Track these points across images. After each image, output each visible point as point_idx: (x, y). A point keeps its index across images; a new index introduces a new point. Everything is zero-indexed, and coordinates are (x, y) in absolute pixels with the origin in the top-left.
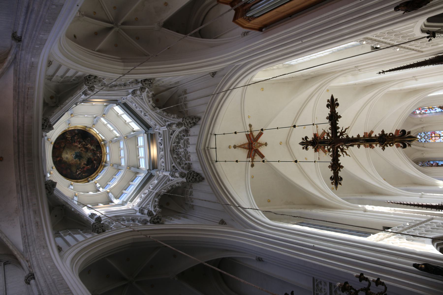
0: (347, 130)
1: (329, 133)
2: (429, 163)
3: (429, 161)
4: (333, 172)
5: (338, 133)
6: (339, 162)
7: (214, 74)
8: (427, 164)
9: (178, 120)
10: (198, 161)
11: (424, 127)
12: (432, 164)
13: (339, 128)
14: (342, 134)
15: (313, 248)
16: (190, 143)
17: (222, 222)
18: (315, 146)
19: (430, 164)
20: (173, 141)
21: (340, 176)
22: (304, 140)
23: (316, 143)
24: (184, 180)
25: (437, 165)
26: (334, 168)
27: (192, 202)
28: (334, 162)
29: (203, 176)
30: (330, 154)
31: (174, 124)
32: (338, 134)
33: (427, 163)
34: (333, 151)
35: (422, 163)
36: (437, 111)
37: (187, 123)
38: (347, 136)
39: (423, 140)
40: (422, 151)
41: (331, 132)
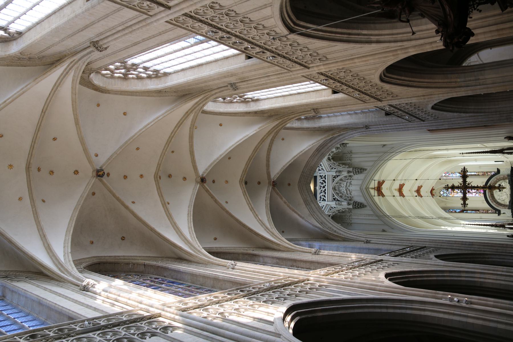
3: (449, 210)
7: (384, 145)
9: (347, 169)
10: (361, 194)
13: (467, 182)
14: (469, 184)
15: (454, 236)
16: (352, 184)
17: (384, 231)
20: (337, 182)
24: (351, 207)
25: (456, 212)
27: (351, 221)
29: (366, 204)
31: (342, 171)
32: (467, 184)
34: (463, 192)
36: (457, 175)
37: (356, 171)
38: (472, 185)
39: (445, 195)
40: (445, 202)
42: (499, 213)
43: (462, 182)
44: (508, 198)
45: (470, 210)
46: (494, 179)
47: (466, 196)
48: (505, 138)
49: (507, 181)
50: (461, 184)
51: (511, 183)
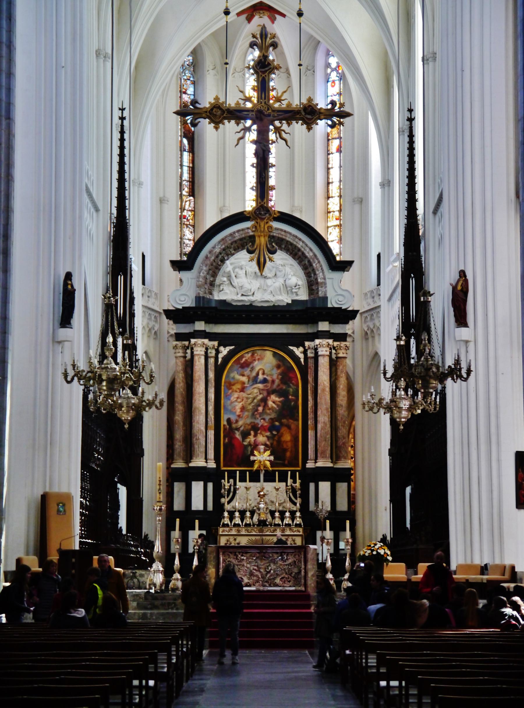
0: (284, 142)
1: (282, 102)
2: (189, 82)
3: (194, 83)
4: (208, 106)
5: (281, 123)
6: (226, 121)
8: (185, 78)
11: (289, 74)
12: (185, 93)
13: (289, 124)
18: (258, 68)
19: (185, 87)
21: (200, 122)
22: (271, 39)
23: (263, 70)
26: (215, 111)
28: (226, 112)
30: (241, 102)
33: (190, 77)
35: (188, 63)
41: (283, 106)
42: (178, 265)
43: (289, 105)
44: (240, 298)
45: (193, 161)
46: (311, 250)
47: (229, 119)
48: (462, 274)
49: (303, 296)
50: (278, 100)
51: (294, 308)
